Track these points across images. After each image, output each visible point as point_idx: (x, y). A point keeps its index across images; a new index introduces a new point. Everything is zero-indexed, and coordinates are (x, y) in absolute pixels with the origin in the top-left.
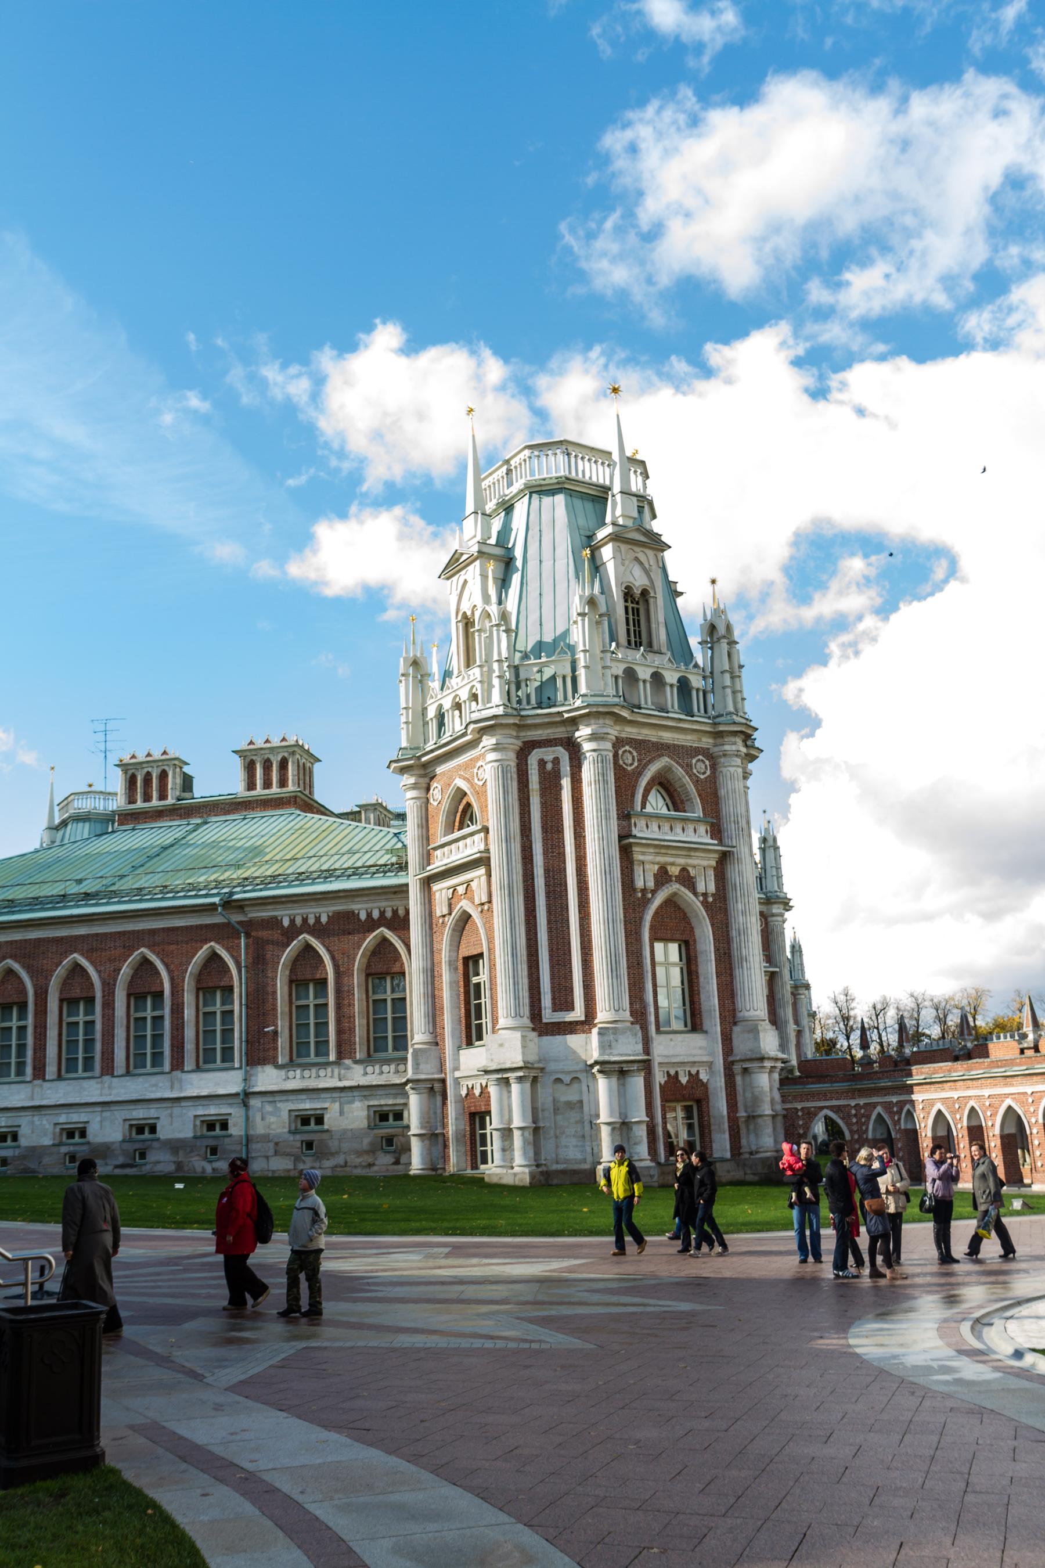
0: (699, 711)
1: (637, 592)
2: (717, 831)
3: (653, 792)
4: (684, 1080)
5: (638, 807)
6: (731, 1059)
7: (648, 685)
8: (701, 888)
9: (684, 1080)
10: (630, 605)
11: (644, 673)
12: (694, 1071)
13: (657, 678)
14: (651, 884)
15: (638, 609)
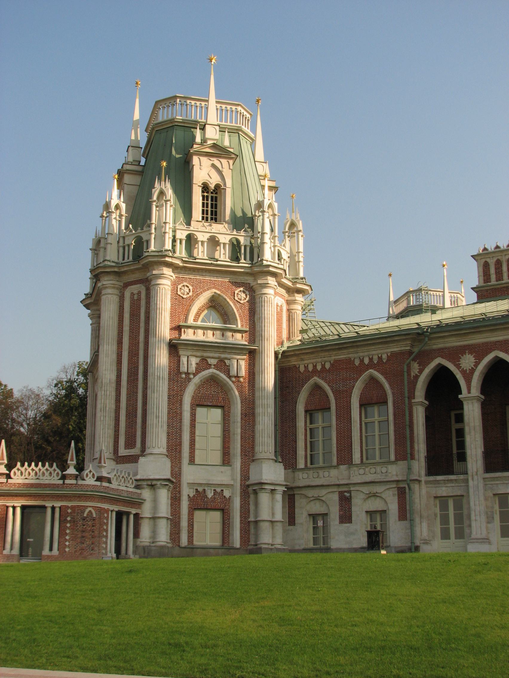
1: (212, 186)
4: (210, 494)
5: (191, 321)
6: (247, 483)
8: (233, 372)
11: (202, 237)
15: (216, 198)
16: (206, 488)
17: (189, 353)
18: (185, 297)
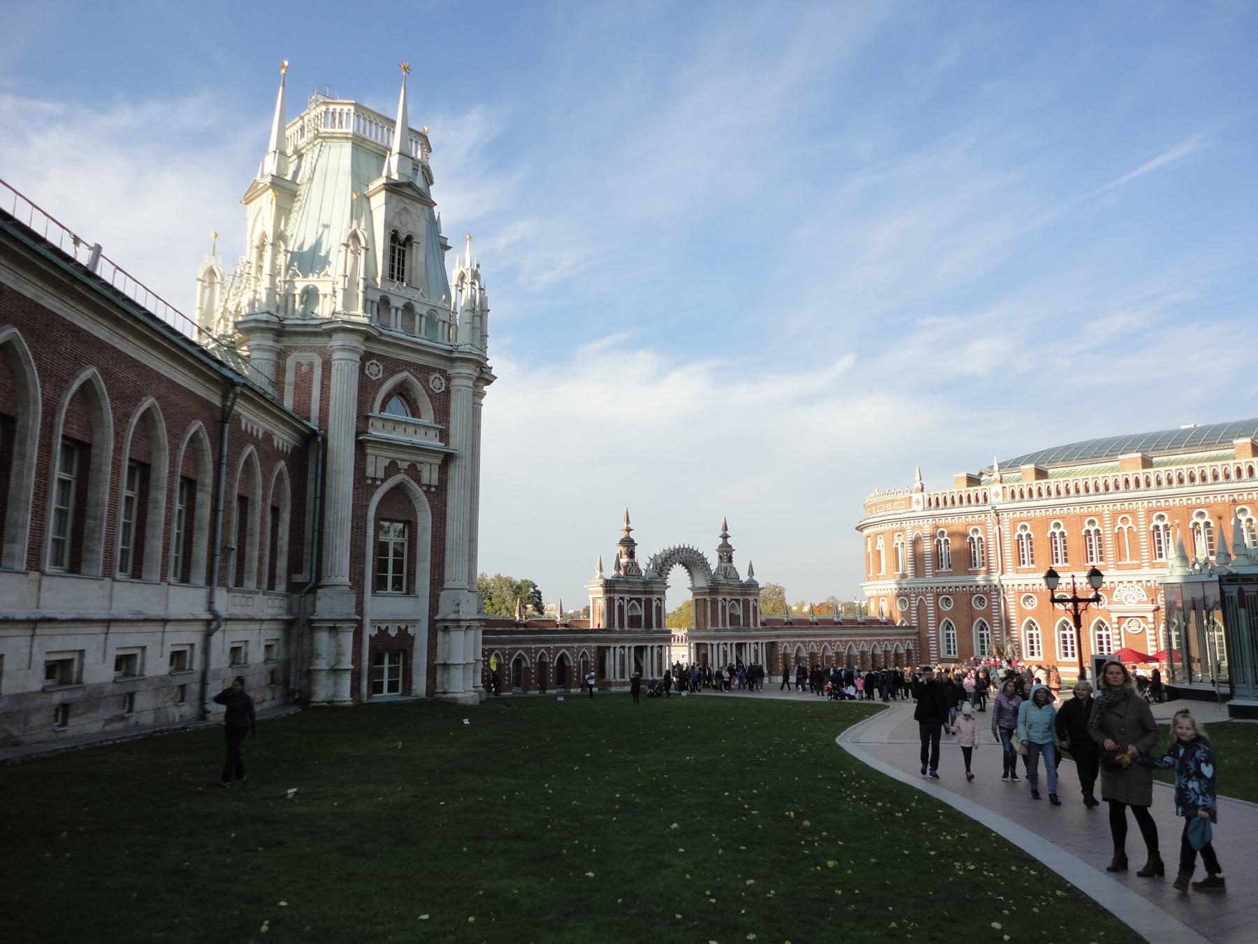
1: (403, 237)
4: (393, 632)
7: (400, 312)
8: (425, 480)
9: (393, 632)
10: (398, 247)
11: (397, 302)
12: (403, 627)
14: (381, 474)
17: (378, 452)
18: (374, 378)
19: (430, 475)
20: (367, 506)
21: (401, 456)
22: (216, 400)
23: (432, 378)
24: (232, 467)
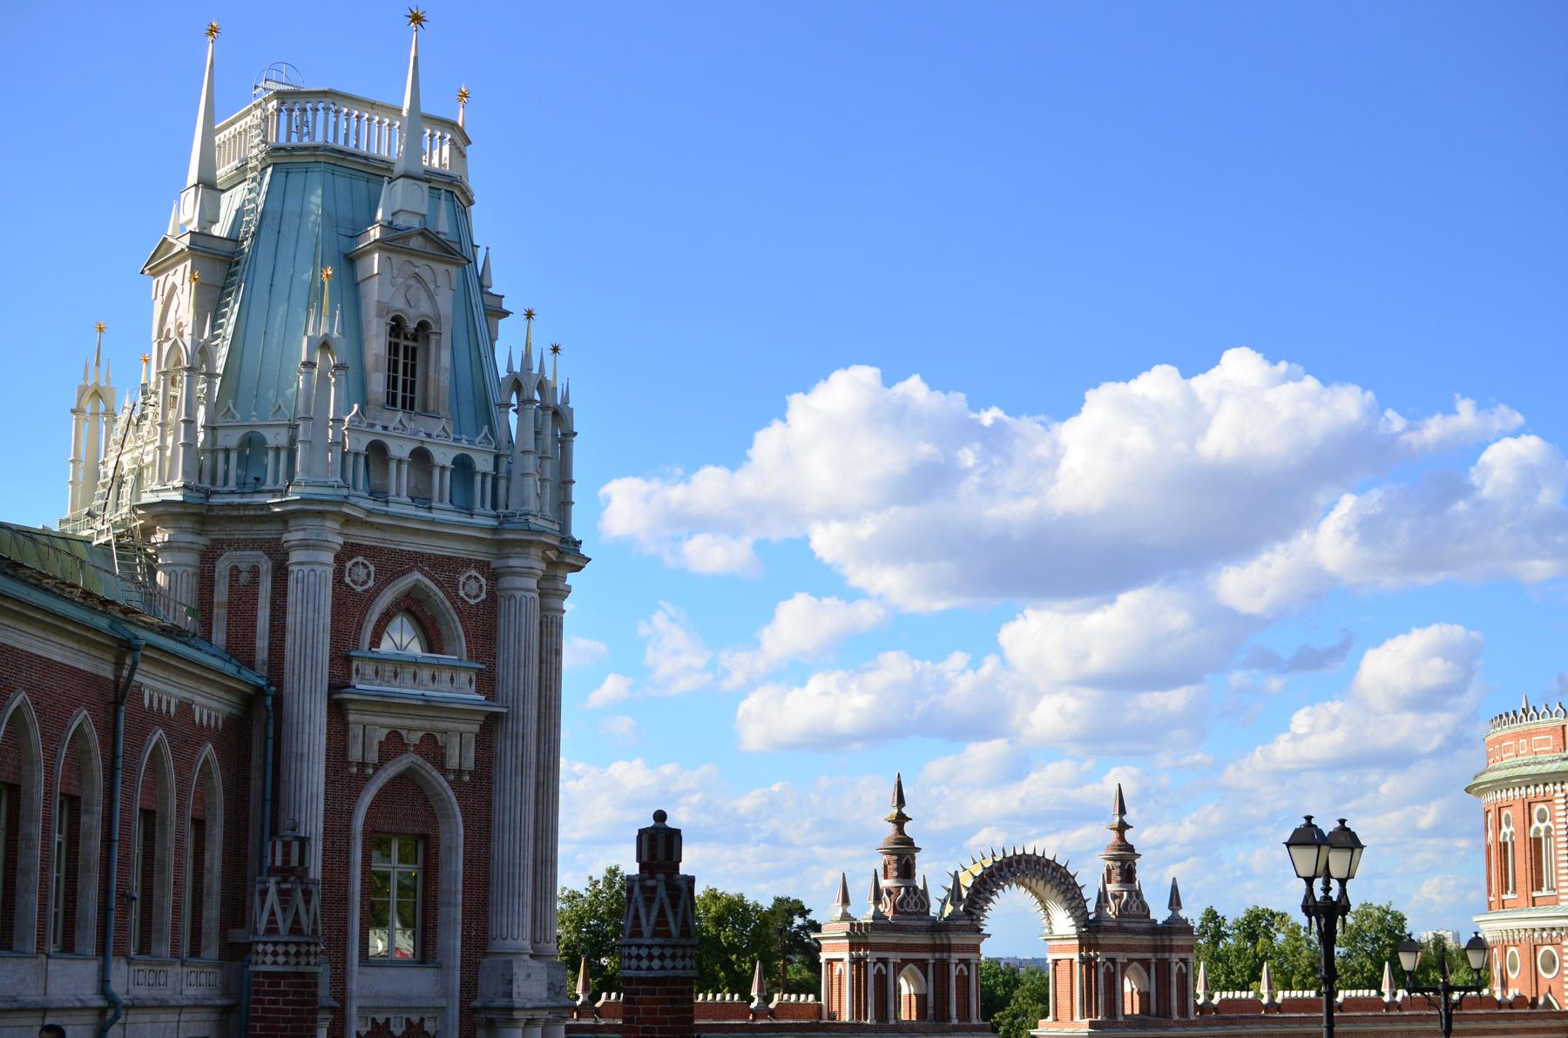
0: (483, 505)
1: (412, 325)
2: (487, 682)
3: (397, 621)
4: (398, 1029)
6: (476, 1004)
7: (405, 467)
8: (453, 763)
9: (398, 1029)
11: (400, 449)
12: (415, 1019)
13: (421, 457)
14: (373, 757)
15: (414, 349)
16: (391, 1016)
17: (367, 719)
18: (359, 589)
19: (462, 755)
20: (350, 813)
21: (408, 722)
22: (107, 671)
23: (462, 579)
24: (131, 770)
